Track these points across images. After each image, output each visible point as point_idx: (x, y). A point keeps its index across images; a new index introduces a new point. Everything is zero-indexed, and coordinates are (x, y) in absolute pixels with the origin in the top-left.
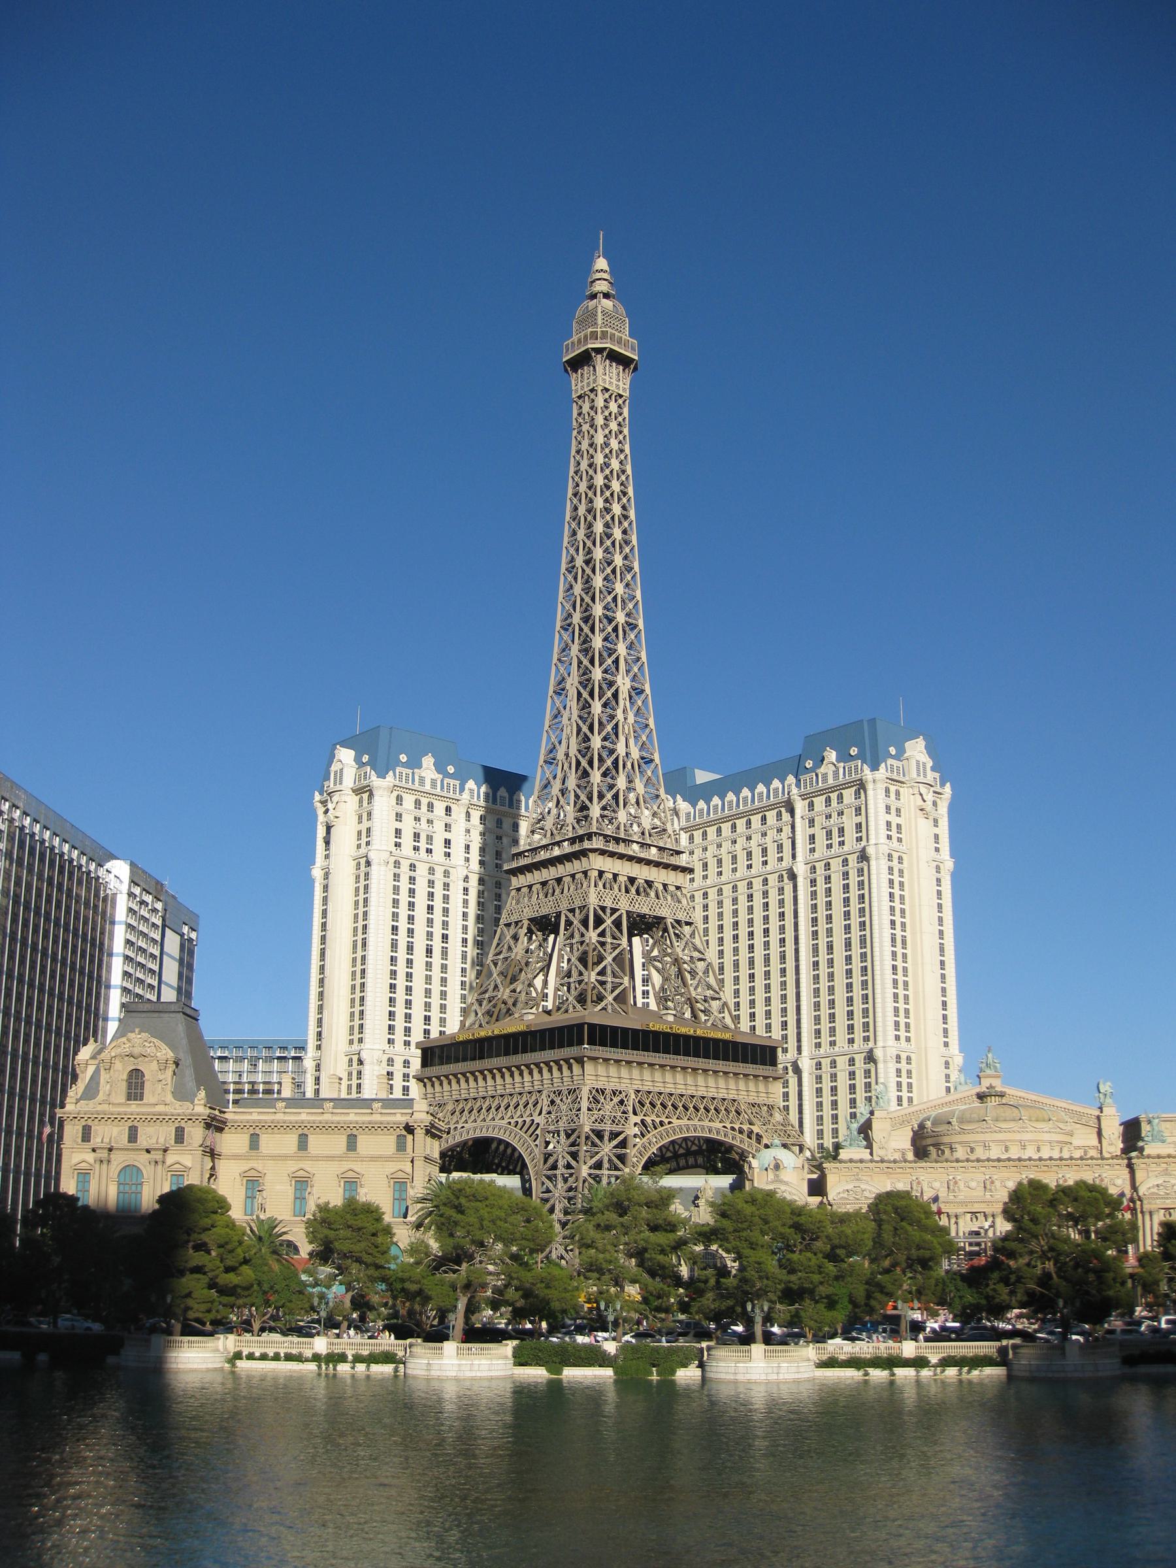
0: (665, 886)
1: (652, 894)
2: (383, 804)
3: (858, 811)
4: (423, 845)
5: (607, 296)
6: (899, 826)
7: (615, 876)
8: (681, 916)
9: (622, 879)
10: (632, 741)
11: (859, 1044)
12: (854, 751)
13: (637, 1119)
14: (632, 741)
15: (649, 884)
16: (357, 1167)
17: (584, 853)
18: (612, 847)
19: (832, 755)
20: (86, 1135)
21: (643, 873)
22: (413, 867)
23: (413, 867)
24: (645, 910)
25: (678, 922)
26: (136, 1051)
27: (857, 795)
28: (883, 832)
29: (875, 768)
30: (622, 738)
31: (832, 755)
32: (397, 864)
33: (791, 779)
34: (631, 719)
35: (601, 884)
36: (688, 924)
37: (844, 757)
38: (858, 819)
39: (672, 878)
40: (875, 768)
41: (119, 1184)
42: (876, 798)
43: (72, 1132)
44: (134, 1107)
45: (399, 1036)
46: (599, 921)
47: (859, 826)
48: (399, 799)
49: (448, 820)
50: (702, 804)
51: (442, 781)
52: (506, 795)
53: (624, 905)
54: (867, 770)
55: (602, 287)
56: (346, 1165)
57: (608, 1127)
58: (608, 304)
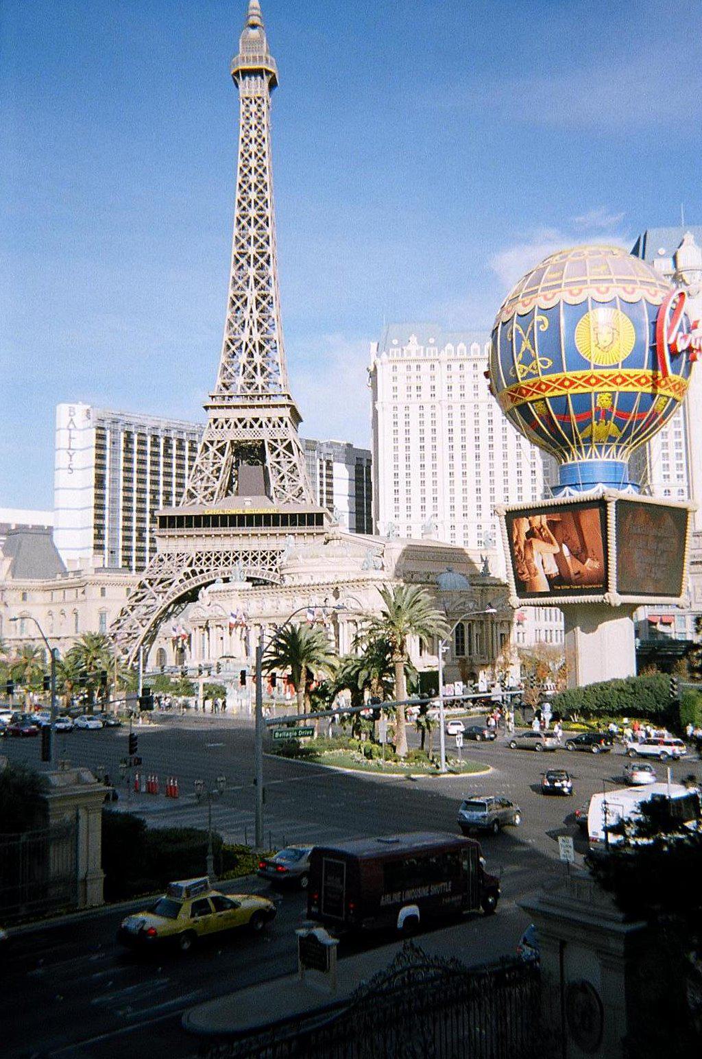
1: (256, 426)
4: (414, 392)
5: (254, 26)
8: (279, 437)
10: (255, 330)
13: (189, 570)
14: (255, 330)
15: (256, 420)
21: (248, 415)
22: (407, 408)
23: (407, 408)
25: (276, 441)
30: (247, 330)
32: (395, 408)
34: (256, 314)
35: (213, 427)
48: (395, 368)
49: (462, 372)
51: (425, 349)
52: (478, 347)
53: (230, 435)
55: (256, 20)
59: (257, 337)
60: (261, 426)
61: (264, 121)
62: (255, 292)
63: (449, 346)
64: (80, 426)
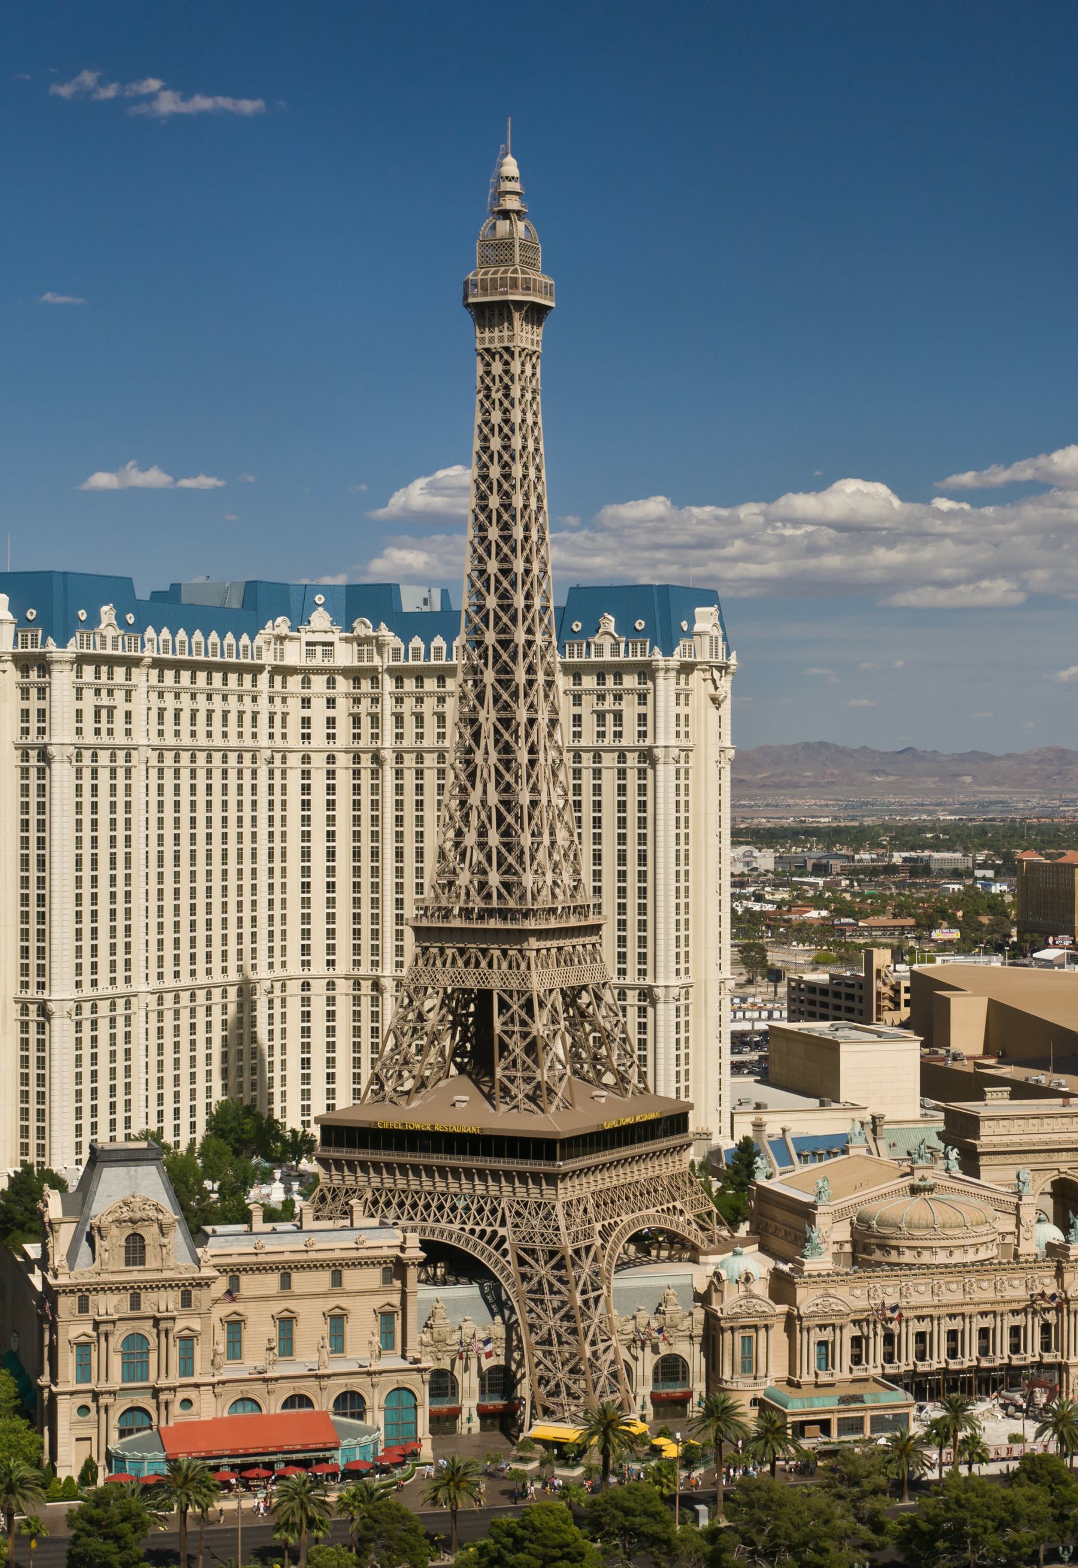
2: (62, 680)
3: (642, 698)
9: (554, 951)
11: (631, 978)
12: (640, 625)
16: (343, 1302)
19: (609, 623)
20: (83, 1307)
26: (138, 1215)
29: (668, 652)
31: (609, 623)
37: (625, 627)
38: (642, 709)
40: (668, 652)
41: (123, 1354)
42: (666, 686)
43: (66, 1305)
44: (135, 1275)
45: (86, 977)
47: (642, 719)
50: (417, 642)
54: (658, 655)
56: (332, 1302)
57: (582, 1244)
63: (150, 632)
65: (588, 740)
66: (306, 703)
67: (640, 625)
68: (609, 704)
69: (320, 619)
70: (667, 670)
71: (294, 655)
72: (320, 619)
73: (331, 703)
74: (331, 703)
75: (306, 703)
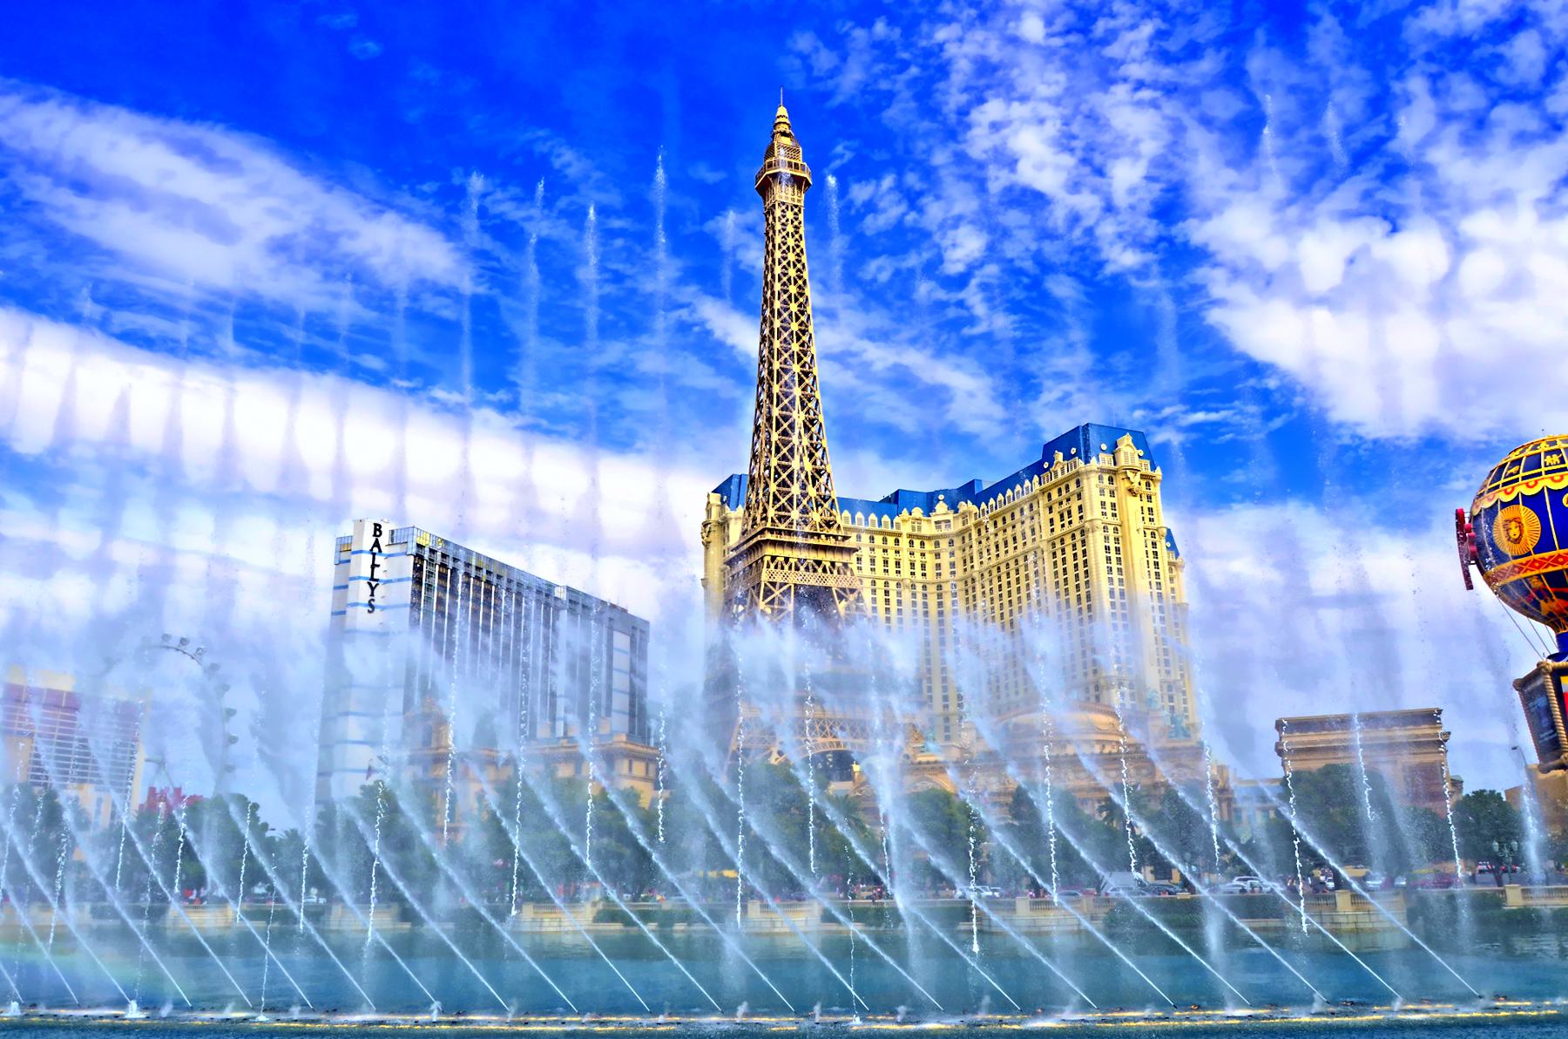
0: (833, 564)
5: (784, 134)
6: (1113, 505)
7: (787, 560)
8: (846, 585)
14: (806, 459)
15: (819, 563)
17: (759, 545)
18: (786, 538)
19: (1059, 456)
24: (813, 582)
25: (844, 590)
27: (1078, 483)
28: (1098, 510)
29: (1087, 462)
30: (797, 457)
31: (1059, 456)
33: (1036, 478)
34: (806, 442)
36: (852, 591)
37: (1068, 457)
39: (839, 559)
46: (768, 593)
47: (1080, 508)
50: (983, 505)
55: (783, 128)
58: (786, 141)
59: (809, 467)
60: (824, 570)
61: (802, 231)
62: (803, 415)
64: (385, 550)
65: (1058, 531)
66: (938, 555)
67: (1073, 451)
68: (1065, 506)
69: (941, 508)
70: (1088, 472)
71: (928, 529)
72: (941, 508)
73: (952, 554)
74: (952, 554)
75: (938, 555)
